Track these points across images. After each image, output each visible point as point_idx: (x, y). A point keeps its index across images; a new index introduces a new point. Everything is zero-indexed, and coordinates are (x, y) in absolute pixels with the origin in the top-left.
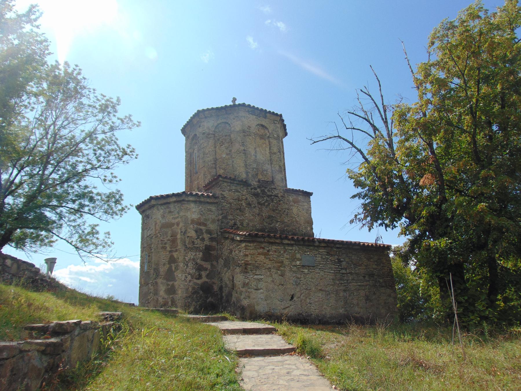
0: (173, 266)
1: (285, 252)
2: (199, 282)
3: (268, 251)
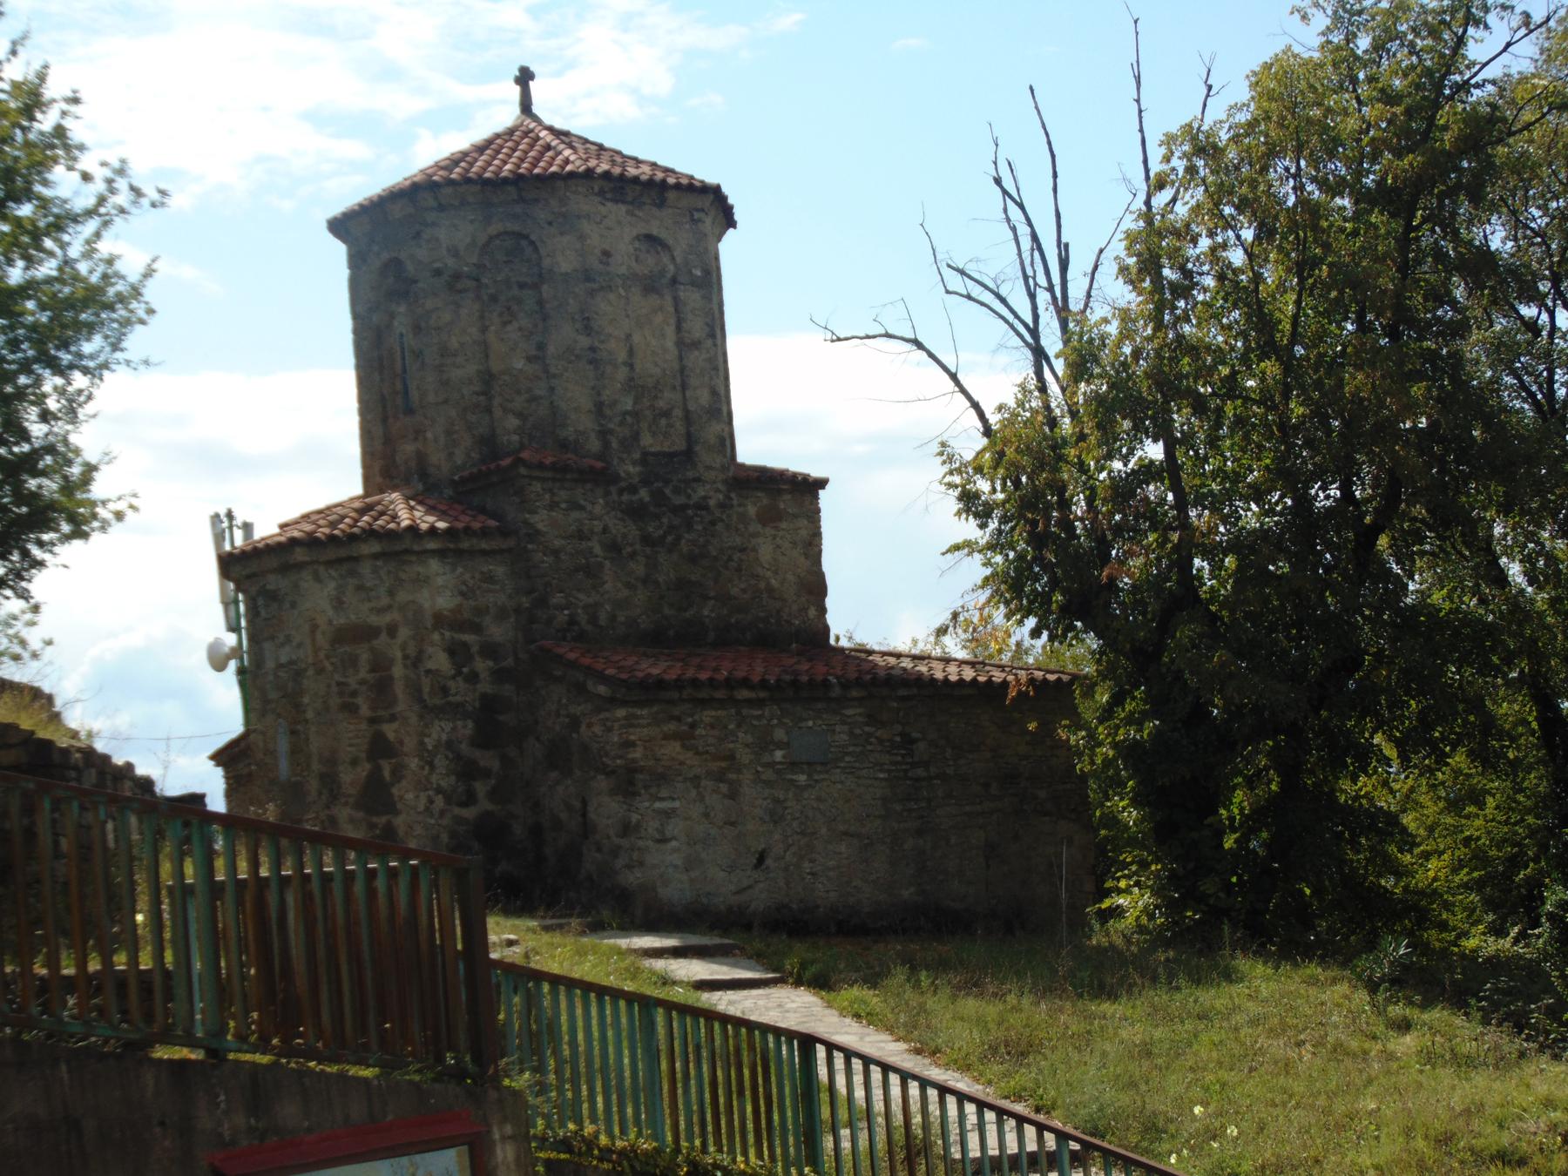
1: (739, 726)
2: (469, 813)
3: (693, 726)
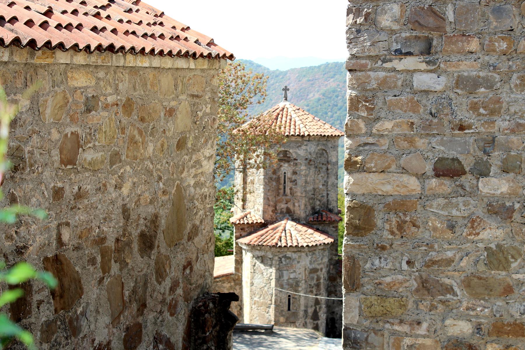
0: (318, 307)
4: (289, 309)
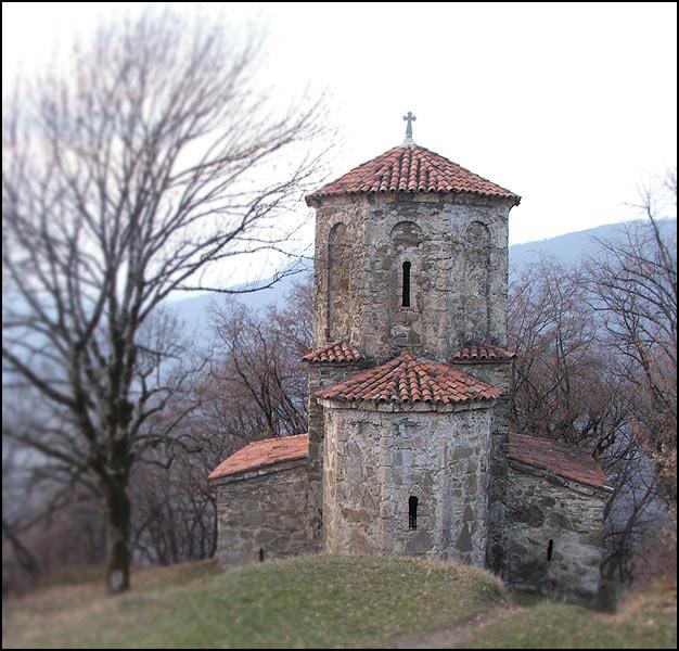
4: (413, 525)
